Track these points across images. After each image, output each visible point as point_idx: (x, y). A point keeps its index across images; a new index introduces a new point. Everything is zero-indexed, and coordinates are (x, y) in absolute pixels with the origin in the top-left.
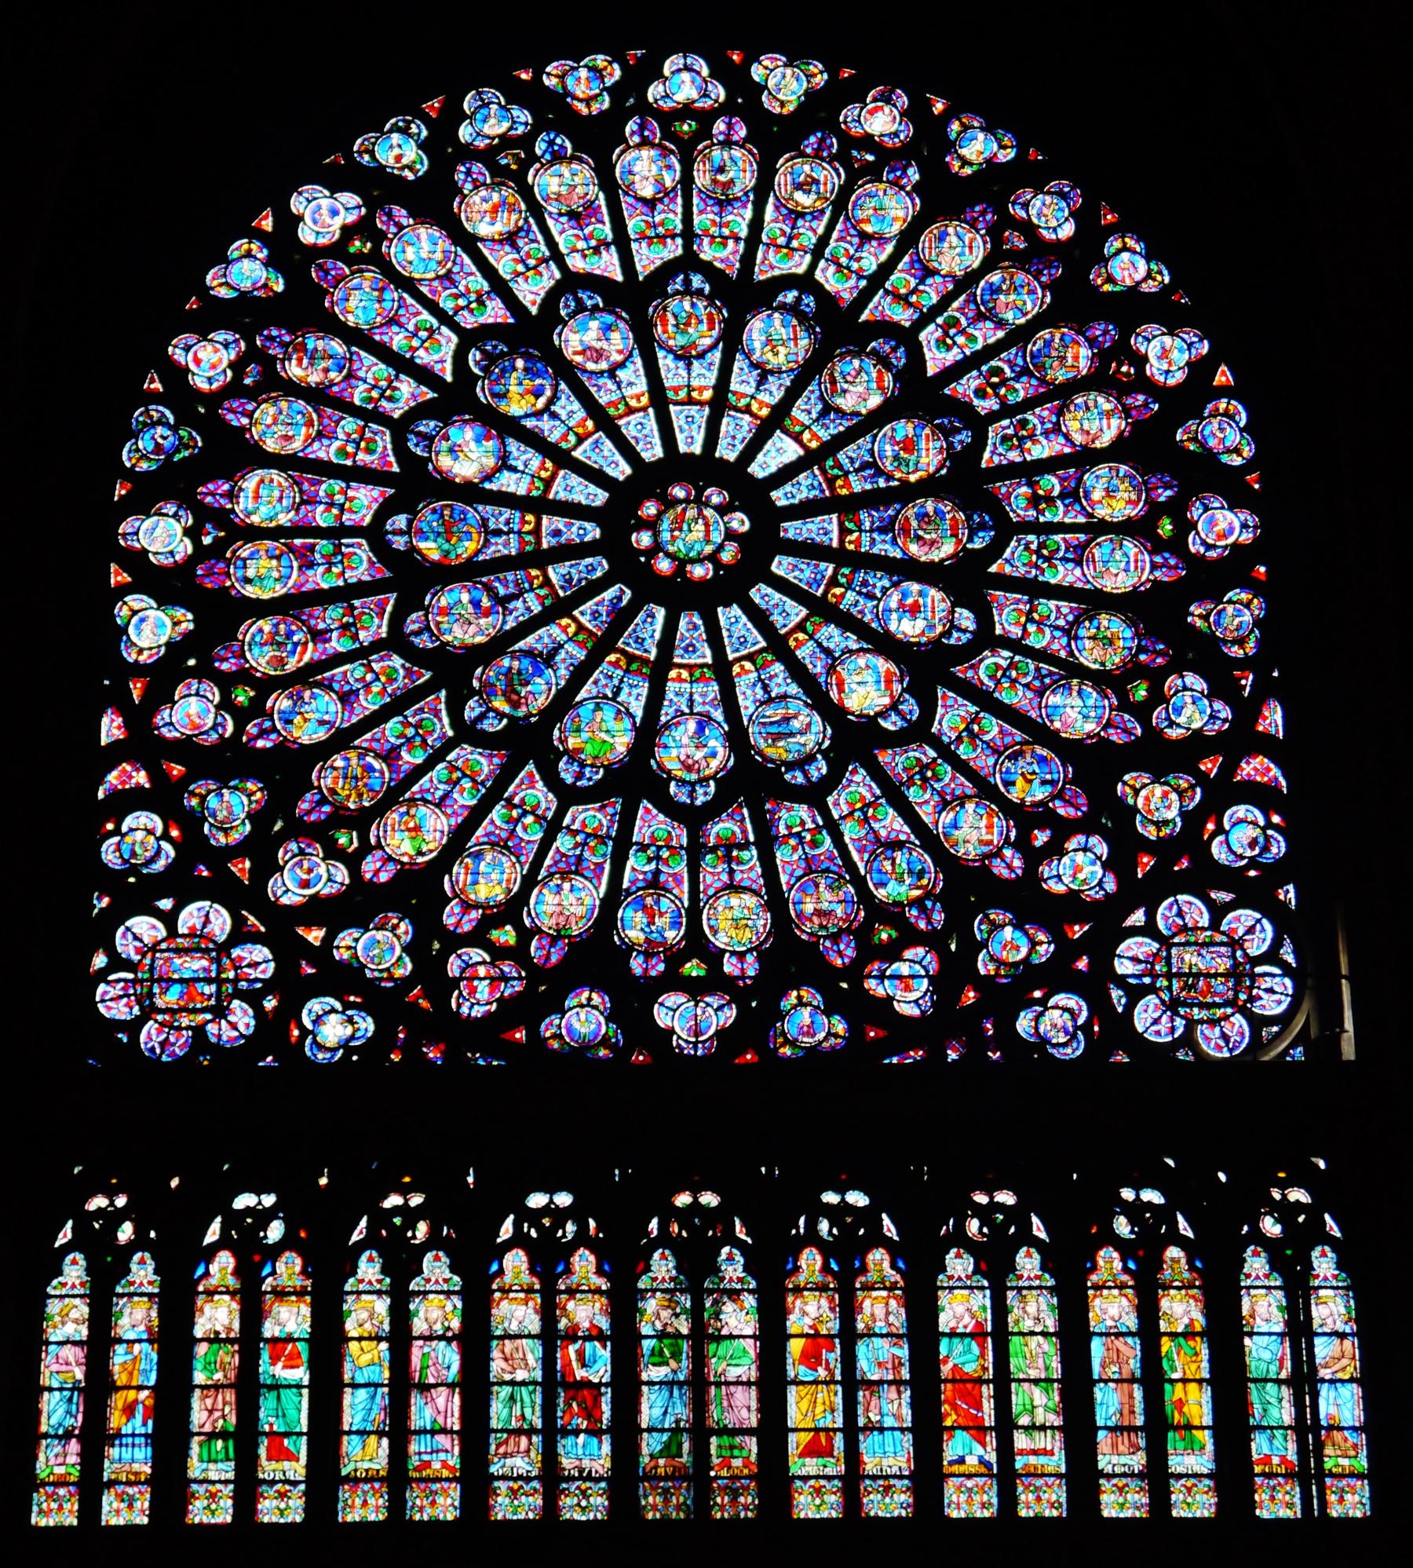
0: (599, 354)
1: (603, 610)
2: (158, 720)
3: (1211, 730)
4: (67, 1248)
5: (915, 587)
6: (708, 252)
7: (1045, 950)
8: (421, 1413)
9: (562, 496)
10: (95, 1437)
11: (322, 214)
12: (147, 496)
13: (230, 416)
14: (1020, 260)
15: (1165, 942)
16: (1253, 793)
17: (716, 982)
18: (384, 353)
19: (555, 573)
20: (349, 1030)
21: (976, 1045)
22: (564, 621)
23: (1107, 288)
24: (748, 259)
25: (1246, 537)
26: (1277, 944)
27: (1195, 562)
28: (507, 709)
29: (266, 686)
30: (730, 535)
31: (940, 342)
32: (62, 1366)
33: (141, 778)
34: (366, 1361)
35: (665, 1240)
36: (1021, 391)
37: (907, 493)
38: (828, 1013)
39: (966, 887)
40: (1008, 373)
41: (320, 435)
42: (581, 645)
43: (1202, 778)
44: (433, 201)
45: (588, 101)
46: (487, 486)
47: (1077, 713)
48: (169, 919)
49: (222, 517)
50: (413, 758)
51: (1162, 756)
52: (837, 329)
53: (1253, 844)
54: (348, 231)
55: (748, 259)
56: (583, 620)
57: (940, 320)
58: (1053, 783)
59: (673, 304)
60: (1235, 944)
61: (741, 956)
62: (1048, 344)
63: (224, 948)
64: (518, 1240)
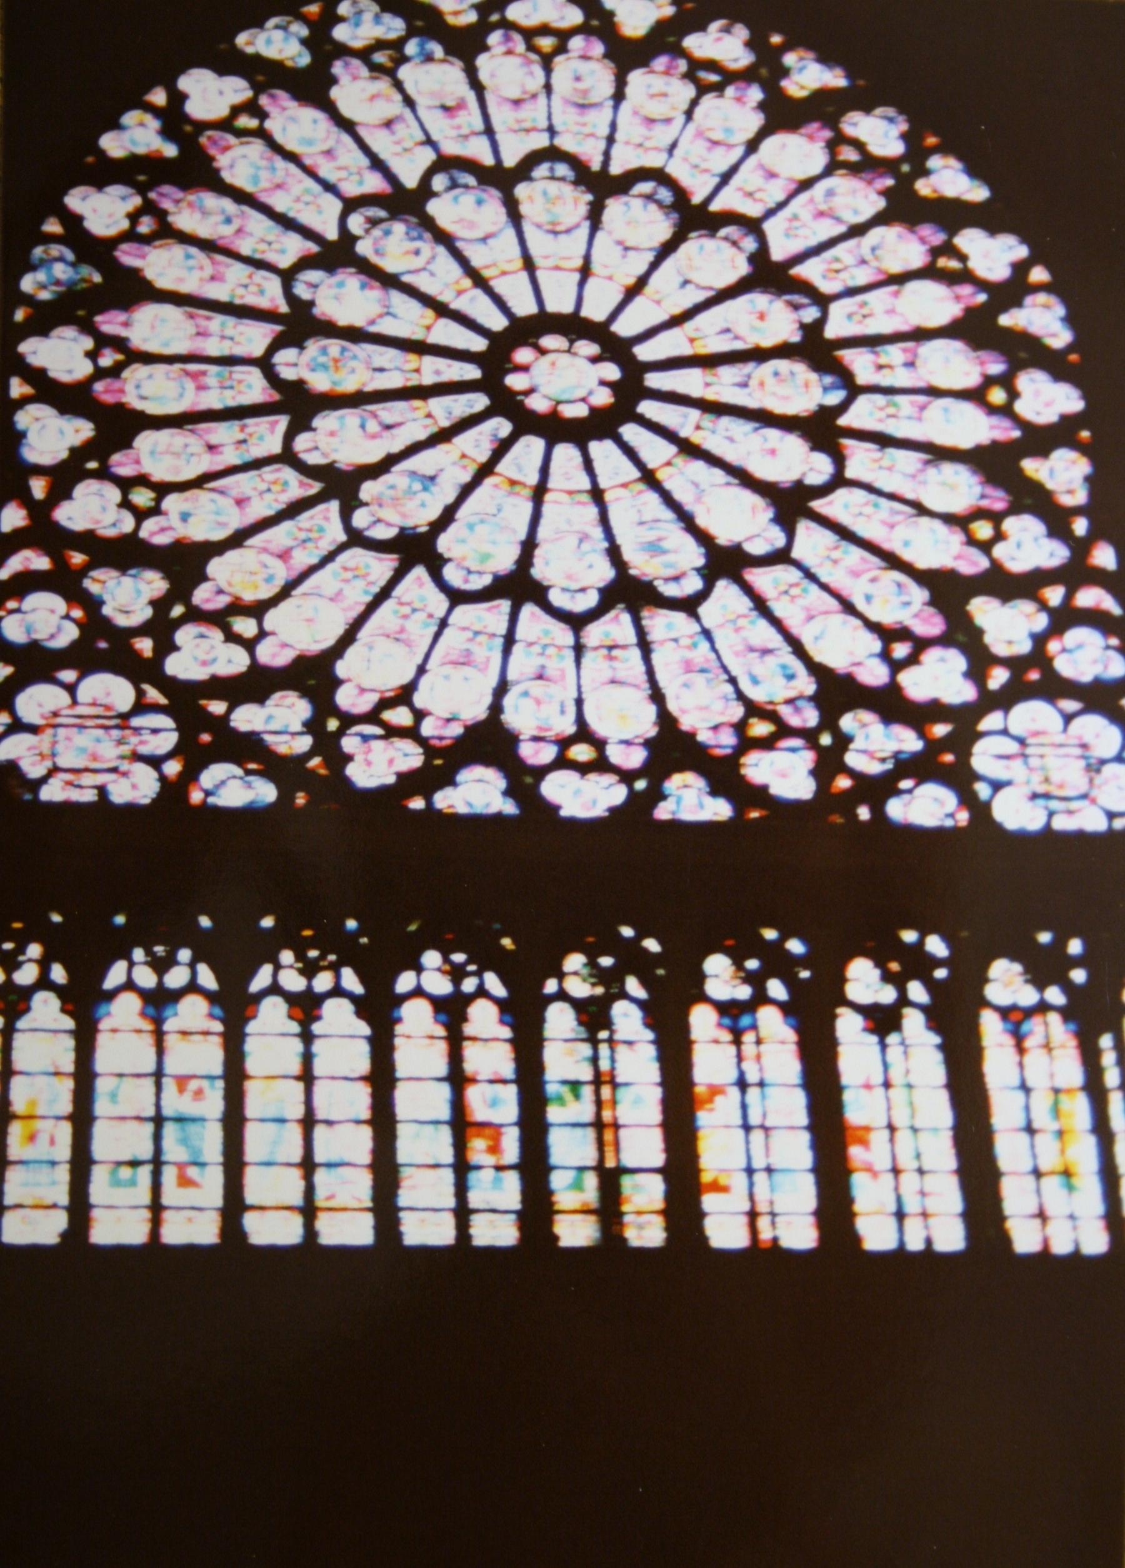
0: (471, 225)
11: (208, 94)
12: (46, 319)
14: (854, 169)
16: (1095, 619)
17: (601, 765)
29: (163, 489)
31: (787, 234)
33: (41, 563)
39: (836, 692)
41: (213, 278)
48: (71, 689)
49: (119, 343)
50: (303, 558)
52: (693, 218)
55: (607, 155)
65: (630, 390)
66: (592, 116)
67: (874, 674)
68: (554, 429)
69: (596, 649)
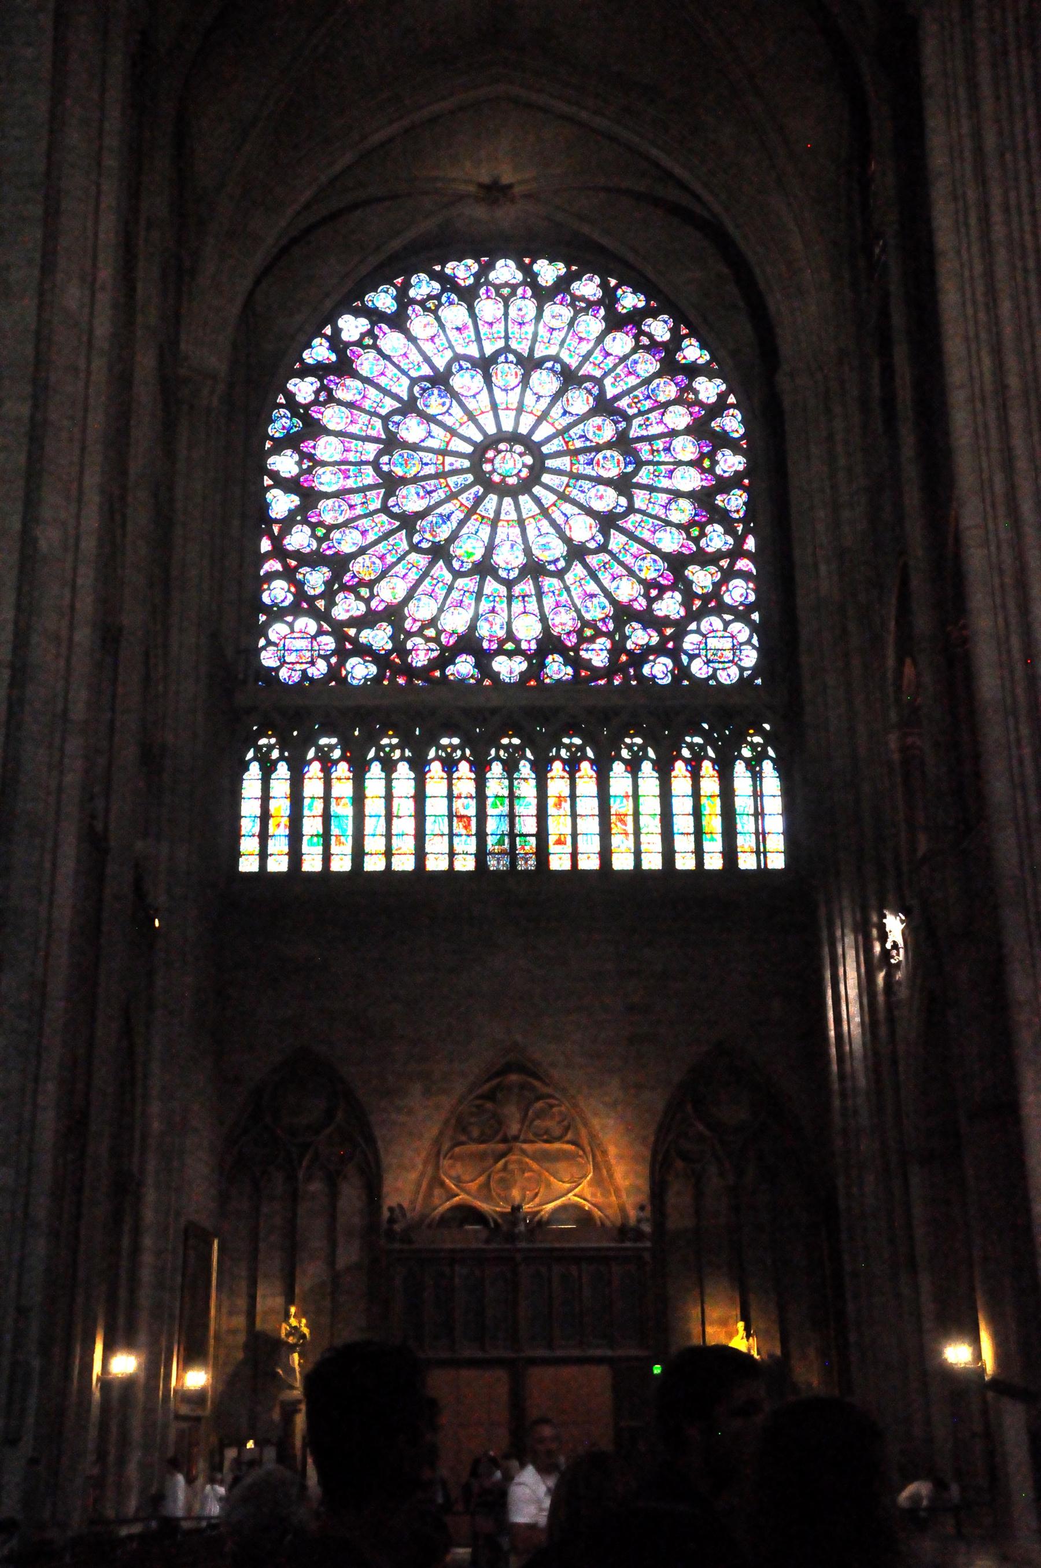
1: (472, 496)
2: (285, 542)
3: (724, 549)
4: (251, 761)
5: (601, 488)
6: (514, 345)
7: (655, 639)
8: (397, 826)
9: (454, 449)
10: (264, 836)
11: (351, 327)
12: (280, 445)
13: (314, 414)
14: (647, 349)
15: (705, 636)
17: (518, 651)
18: (377, 386)
19: (452, 481)
20: (364, 672)
21: (627, 679)
22: (455, 501)
23: (683, 361)
24: (532, 350)
25: (741, 468)
26: (751, 637)
27: (719, 478)
28: (431, 538)
29: (330, 528)
30: (524, 465)
32: (250, 808)
34: (374, 806)
35: (497, 758)
36: (647, 404)
37: (598, 448)
38: (565, 665)
39: (623, 614)
40: (641, 398)
42: (462, 511)
43: (721, 568)
44: (398, 321)
45: (464, 279)
46: (422, 444)
47: (670, 541)
48: (291, 625)
49: (311, 457)
50: (390, 559)
51: (704, 559)
52: (570, 378)
53: (742, 595)
54: (363, 336)
55: (532, 350)
56: (464, 502)
57: (613, 375)
58: (659, 570)
59: (500, 367)
60: (733, 637)
61: (529, 642)
62: (658, 385)
63: (314, 638)
64: (438, 758)
65: (537, 470)
66: (525, 328)
67: (641, 604)
68: (503, 490)
69: (517, 597)
